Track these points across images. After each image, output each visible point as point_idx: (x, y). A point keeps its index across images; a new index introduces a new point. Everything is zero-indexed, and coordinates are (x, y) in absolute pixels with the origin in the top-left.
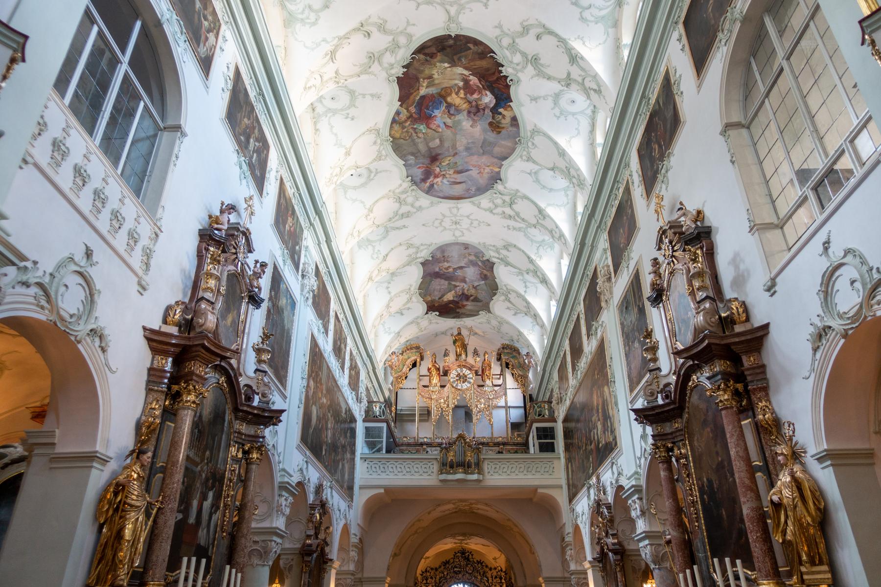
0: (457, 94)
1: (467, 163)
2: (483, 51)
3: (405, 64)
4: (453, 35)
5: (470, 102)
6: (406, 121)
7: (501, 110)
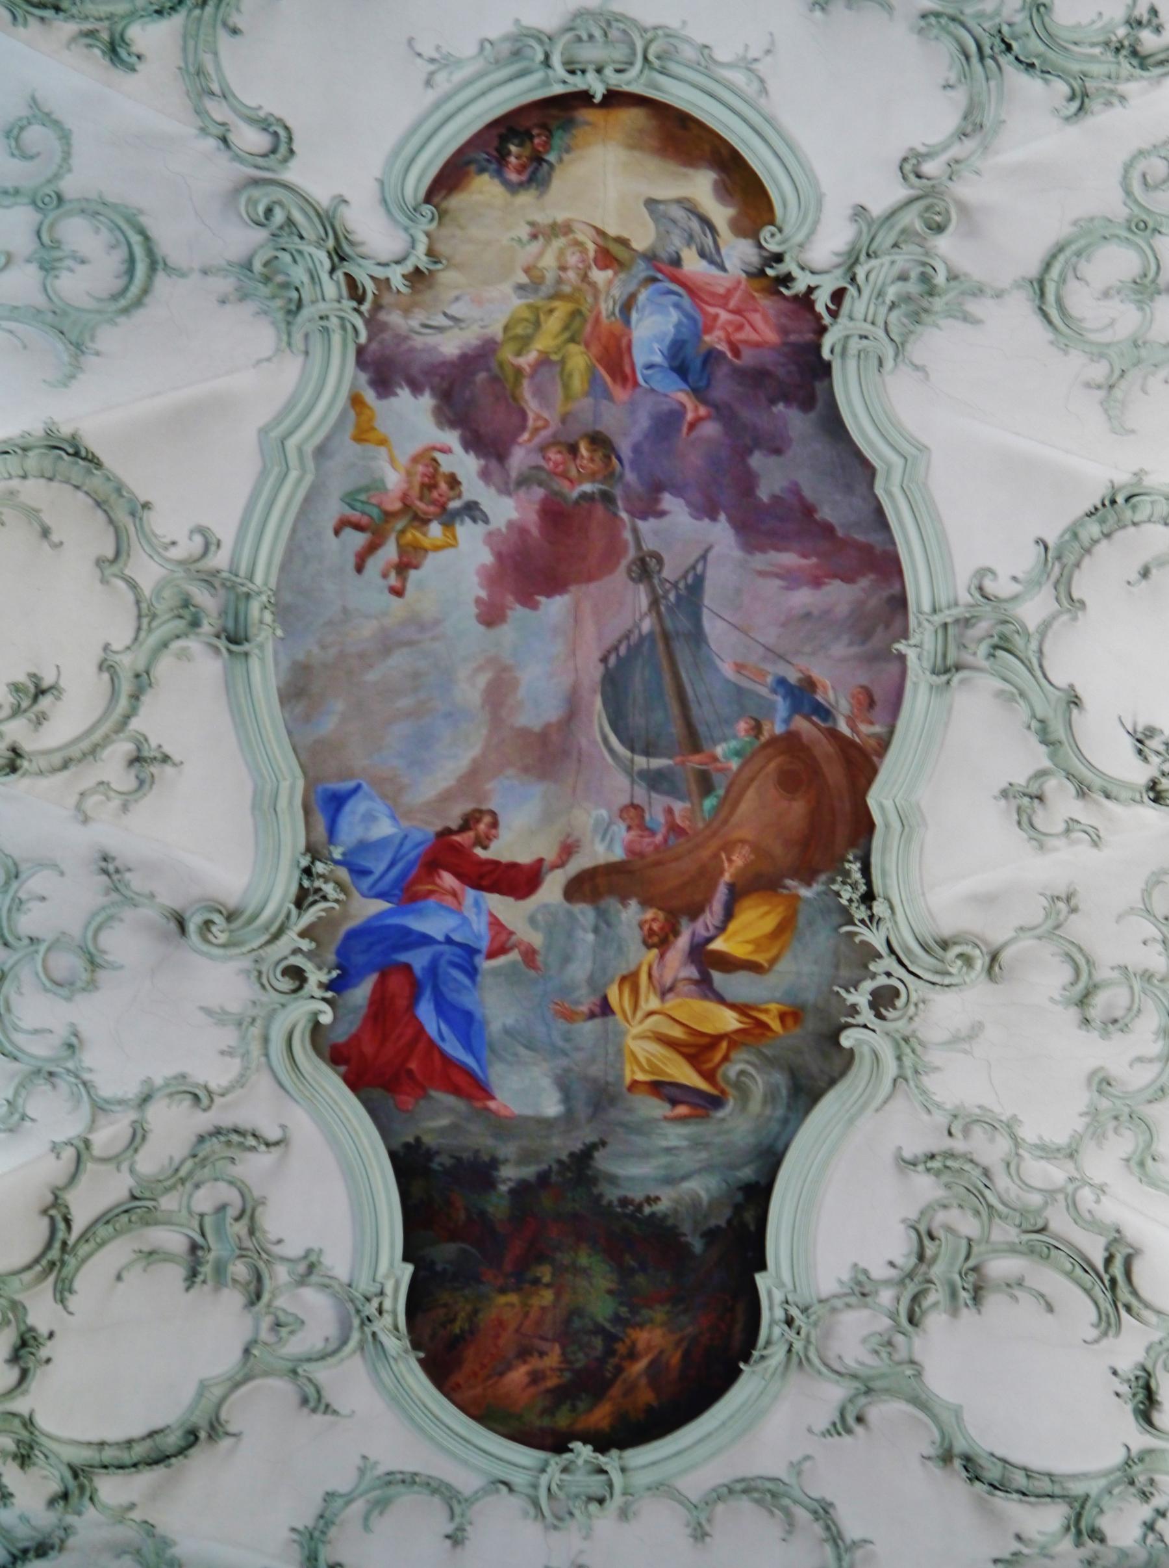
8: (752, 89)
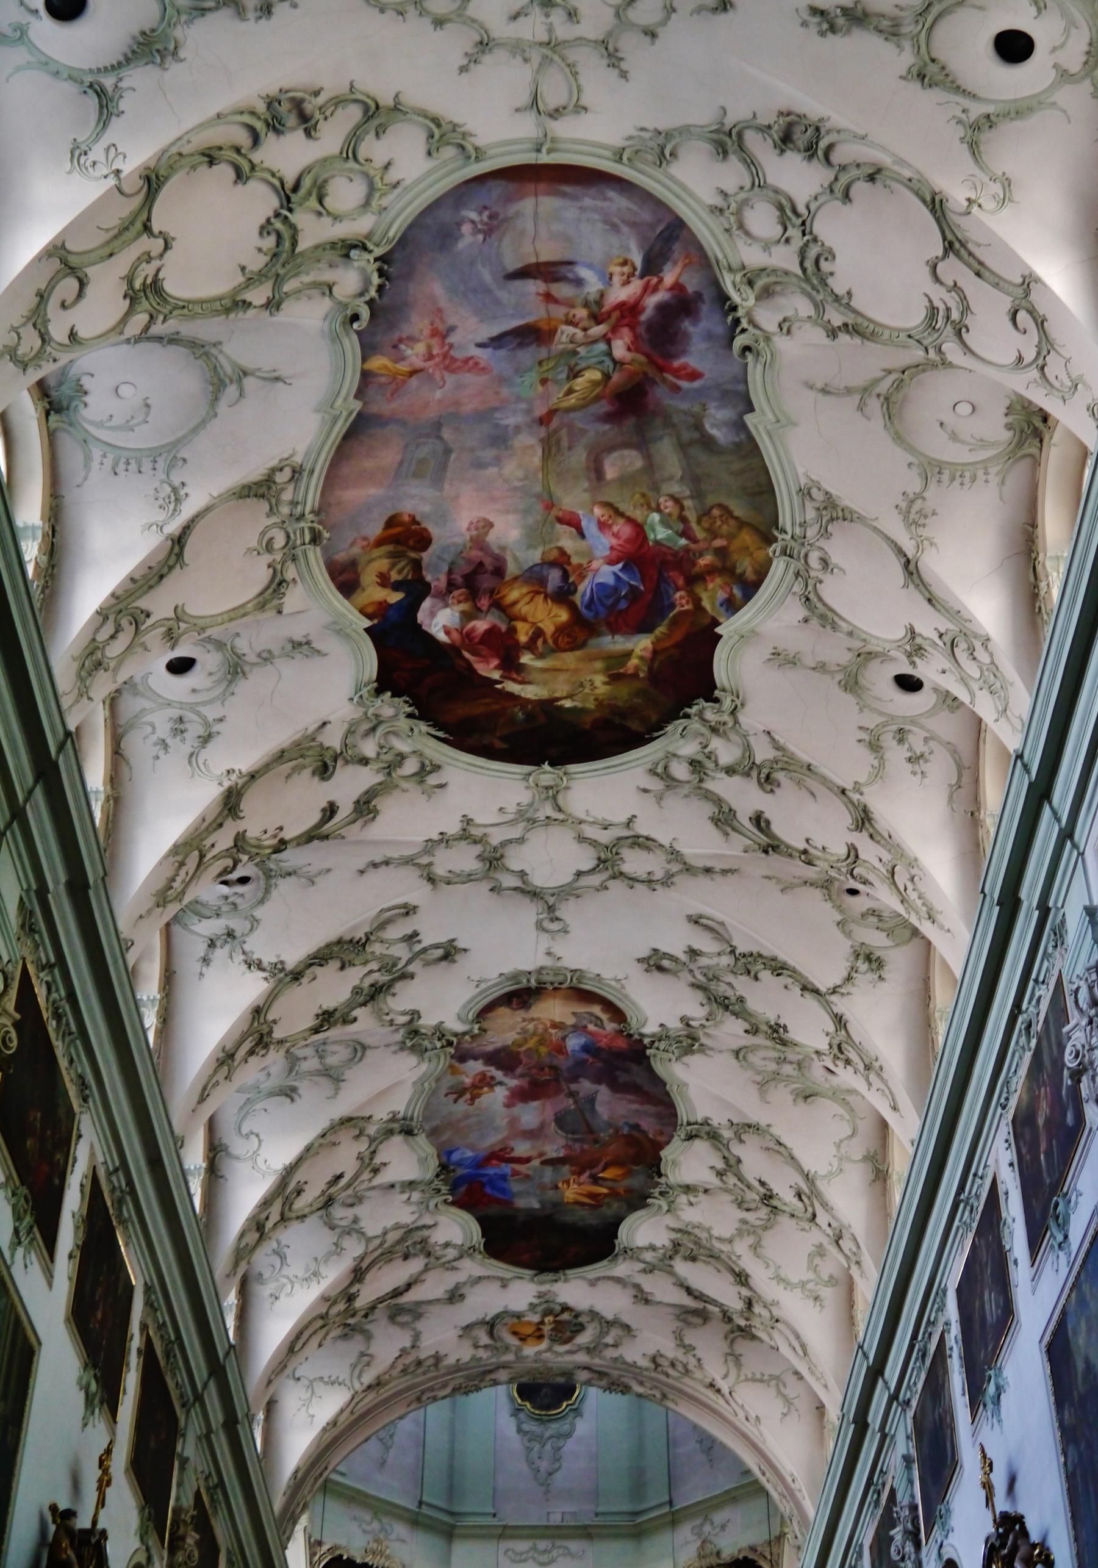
1: (502, 380)
3: (681, 723)
4: (546, 767)
5: (498, 605)
6: (711, 571)
7: (395, 597)
8: (618, 986)
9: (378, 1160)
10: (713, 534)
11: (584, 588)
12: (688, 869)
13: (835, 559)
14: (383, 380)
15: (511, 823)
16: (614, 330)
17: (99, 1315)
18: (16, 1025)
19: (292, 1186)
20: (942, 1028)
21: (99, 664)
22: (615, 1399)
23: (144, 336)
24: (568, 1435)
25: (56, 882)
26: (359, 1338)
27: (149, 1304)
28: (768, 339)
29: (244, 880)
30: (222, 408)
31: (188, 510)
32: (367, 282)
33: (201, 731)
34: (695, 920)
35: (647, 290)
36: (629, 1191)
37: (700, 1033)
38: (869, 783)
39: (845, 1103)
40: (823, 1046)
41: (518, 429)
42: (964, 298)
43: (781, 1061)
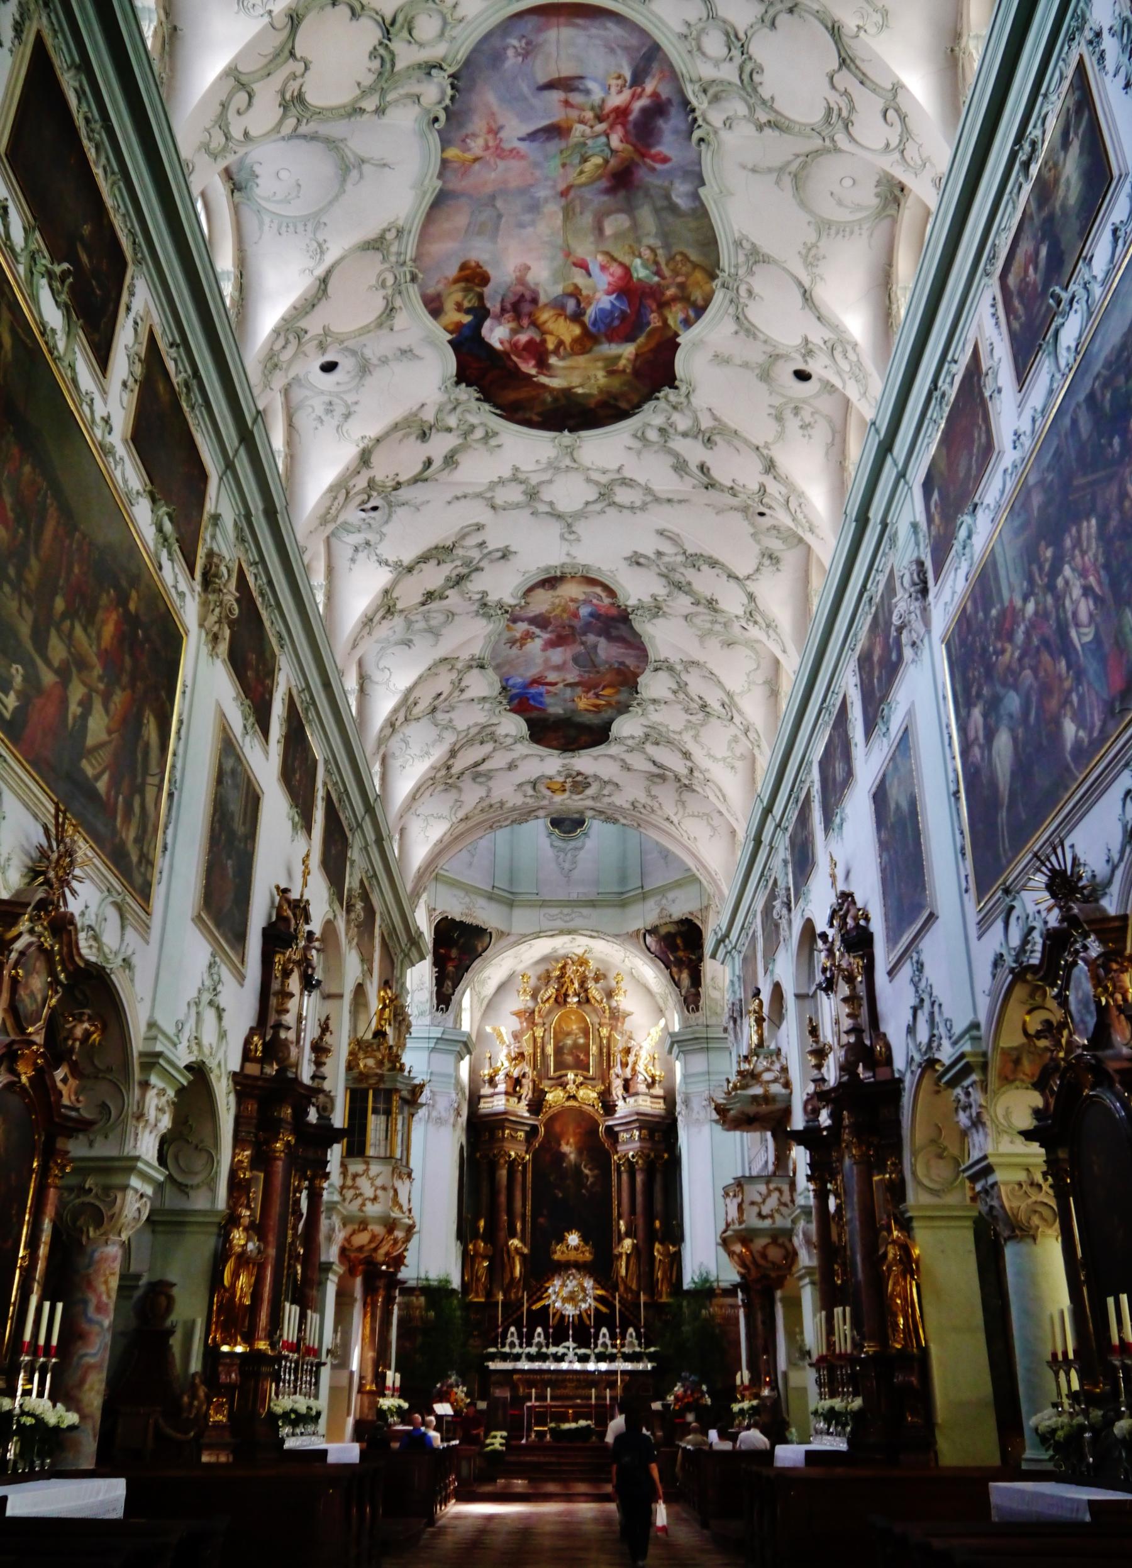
0: (560, 343)
1: (536, 165)
2: (515, 413)
3: (653, 403)
4: (566, 432)
5: (534, 324)
6: (674, 299)
7: (467, 319)
9: (463, 684)
10: (676, 273)
11: (591, 313)
12: (657, 500)
13: (757, 289)
14: (456, 165)
15: (544, 470)
16: (612, 127)
17: (297, 776)
18: (238, 600)
19: (411, 700)
20: (815, 601)
21: (276, 366)
22: (610, 827)
23: (295, 135)
24: (581, 848)
25: (256, 508)
26: (454, 791)
27: (328, 771)
28: (716, 132)
29: (375, 509)
30: (349, 186)
31: (330, 259)
32: (443, 93)
33: (344, 411)
34: (661, 533)
35: (635, 97)
36: (618, 703)
37: (663, 605)
38: (774, 443)
39: (753, 649)
40: (740, 612)
41: (546, 200)
42: (851, 101)
43: (714, 622)
